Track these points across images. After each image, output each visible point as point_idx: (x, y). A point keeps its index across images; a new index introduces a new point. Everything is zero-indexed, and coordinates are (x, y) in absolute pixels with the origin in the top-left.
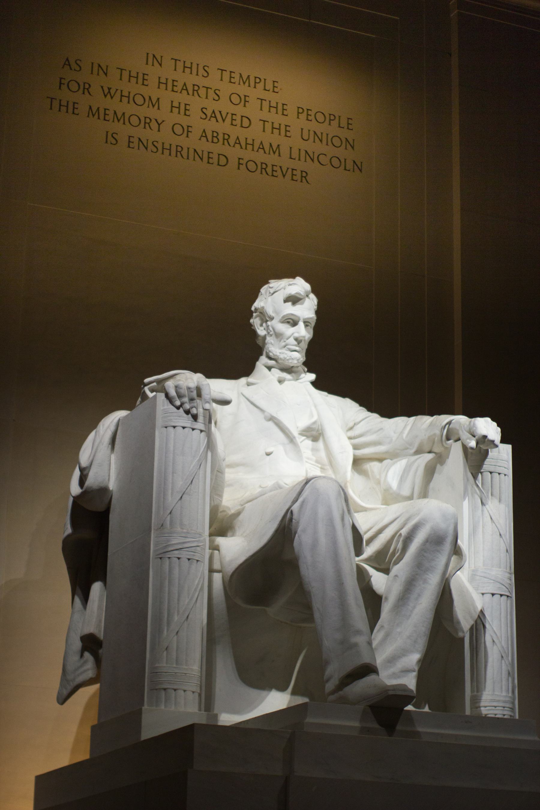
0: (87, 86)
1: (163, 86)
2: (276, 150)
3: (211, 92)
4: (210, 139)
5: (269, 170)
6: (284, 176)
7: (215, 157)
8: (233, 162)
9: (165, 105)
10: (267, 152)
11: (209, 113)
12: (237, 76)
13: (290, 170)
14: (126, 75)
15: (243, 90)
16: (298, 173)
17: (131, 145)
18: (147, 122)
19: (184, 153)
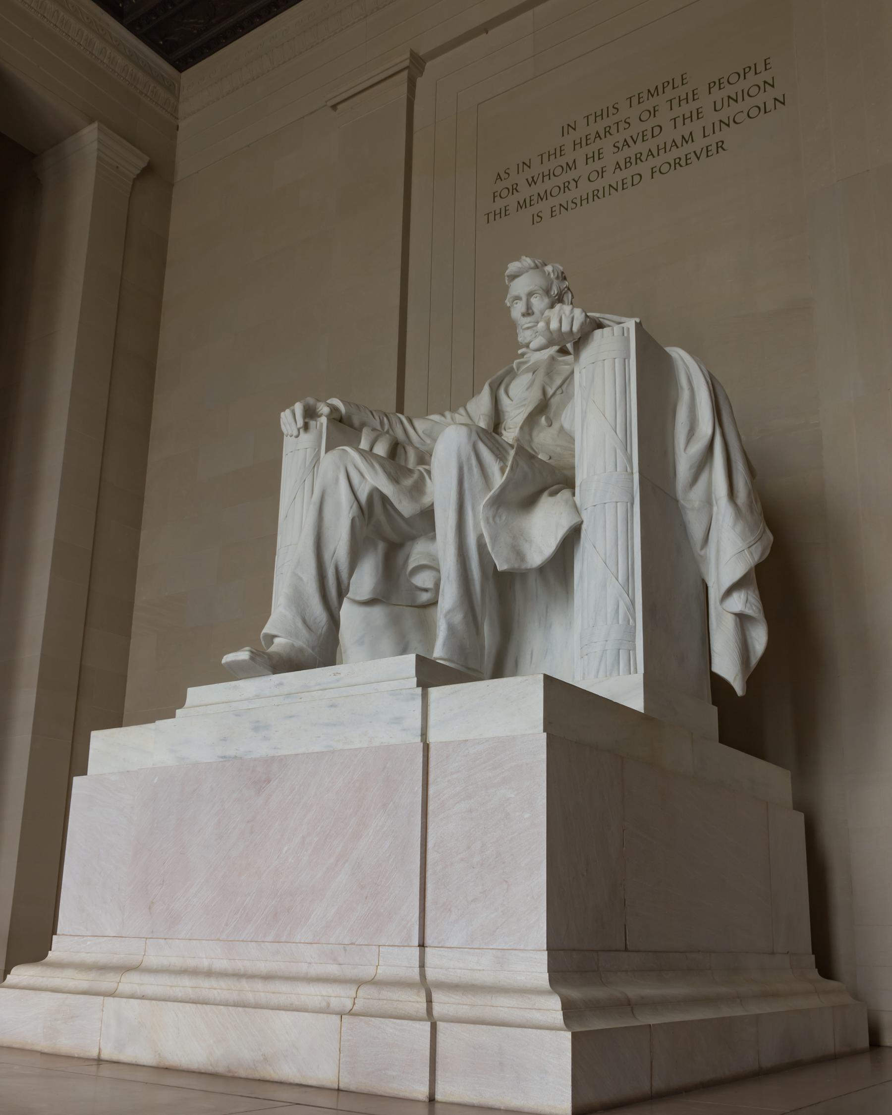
0: (515, 186)
1: (578, 147)
2: (688, 139)
3: (622, 125)
4: (623, 167)
5: (683, 162)
6: (698, 158)
7: (629, 181)
8: (647, 174)
9: (581, 162)
10: (679, 145)
11: (620, 145)
12: (645, 95)
13: (705, 150)
14: (545, 157)
15: (649, 104)
16: (714, 148)
17: (554, 214)
18: (566, 187)
19: (600, 194)
